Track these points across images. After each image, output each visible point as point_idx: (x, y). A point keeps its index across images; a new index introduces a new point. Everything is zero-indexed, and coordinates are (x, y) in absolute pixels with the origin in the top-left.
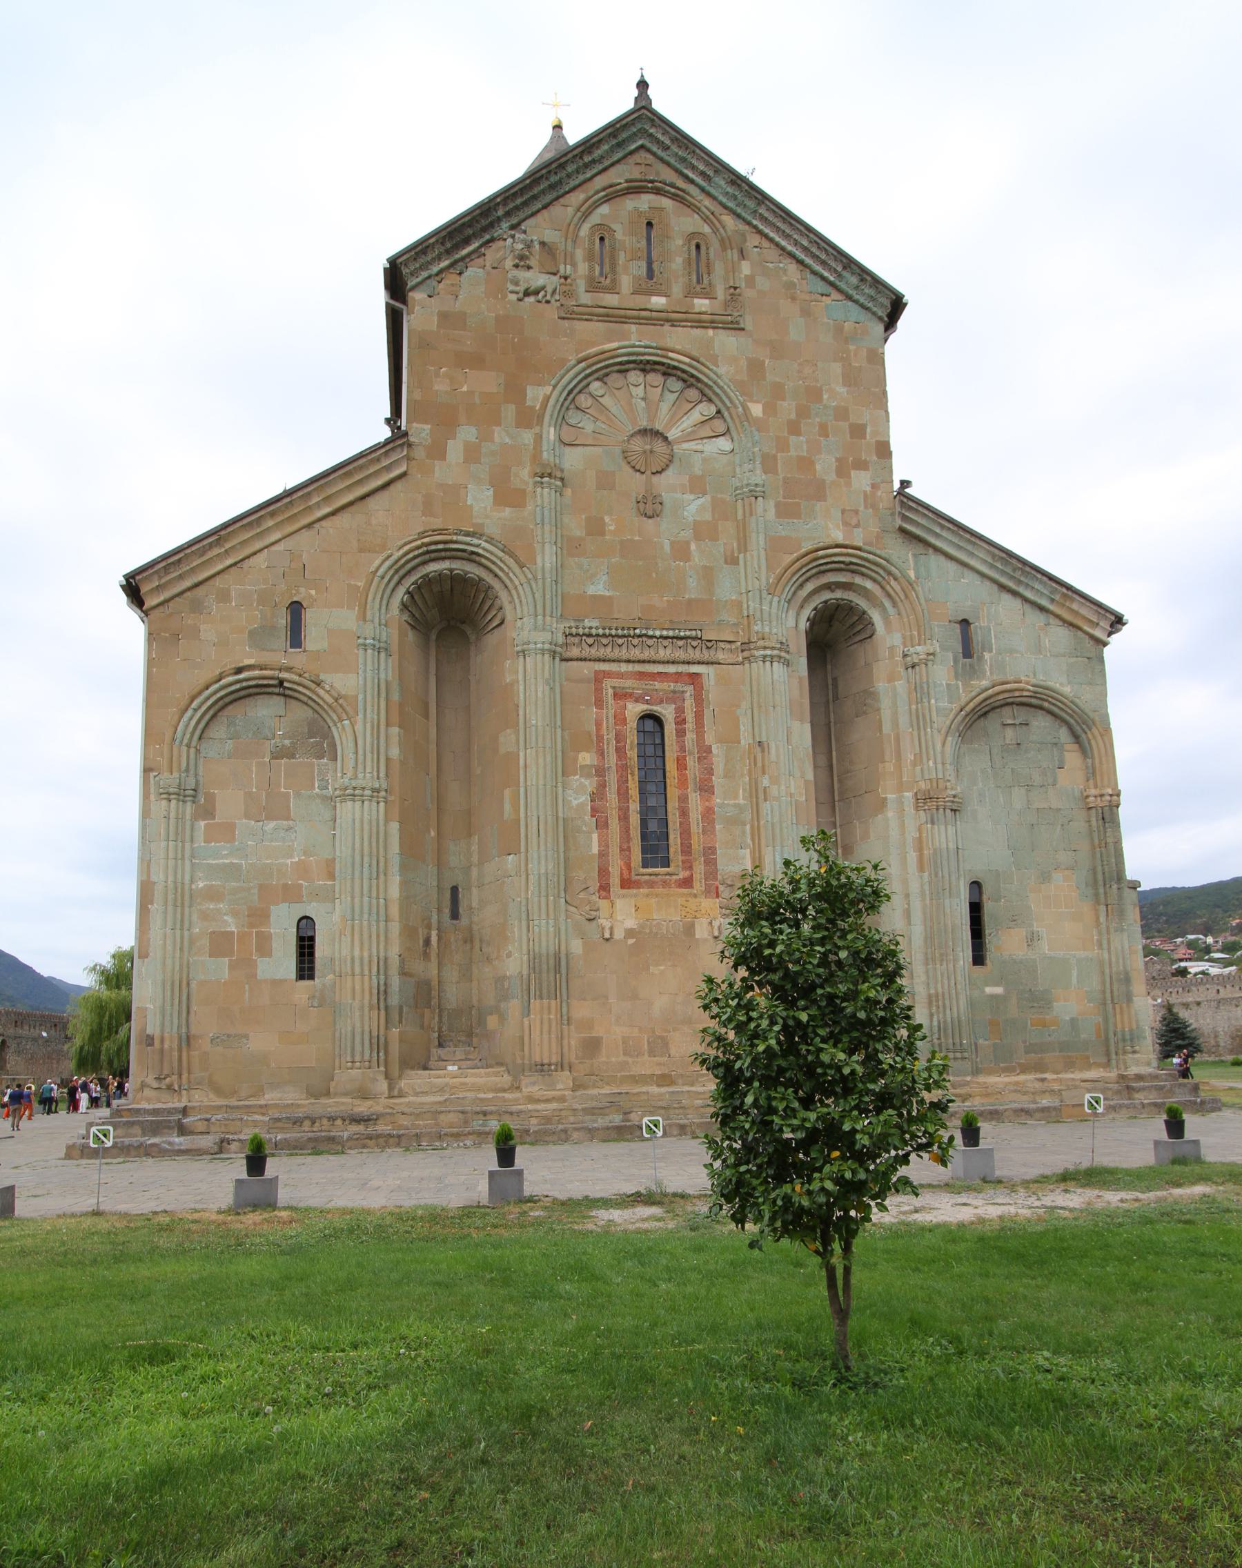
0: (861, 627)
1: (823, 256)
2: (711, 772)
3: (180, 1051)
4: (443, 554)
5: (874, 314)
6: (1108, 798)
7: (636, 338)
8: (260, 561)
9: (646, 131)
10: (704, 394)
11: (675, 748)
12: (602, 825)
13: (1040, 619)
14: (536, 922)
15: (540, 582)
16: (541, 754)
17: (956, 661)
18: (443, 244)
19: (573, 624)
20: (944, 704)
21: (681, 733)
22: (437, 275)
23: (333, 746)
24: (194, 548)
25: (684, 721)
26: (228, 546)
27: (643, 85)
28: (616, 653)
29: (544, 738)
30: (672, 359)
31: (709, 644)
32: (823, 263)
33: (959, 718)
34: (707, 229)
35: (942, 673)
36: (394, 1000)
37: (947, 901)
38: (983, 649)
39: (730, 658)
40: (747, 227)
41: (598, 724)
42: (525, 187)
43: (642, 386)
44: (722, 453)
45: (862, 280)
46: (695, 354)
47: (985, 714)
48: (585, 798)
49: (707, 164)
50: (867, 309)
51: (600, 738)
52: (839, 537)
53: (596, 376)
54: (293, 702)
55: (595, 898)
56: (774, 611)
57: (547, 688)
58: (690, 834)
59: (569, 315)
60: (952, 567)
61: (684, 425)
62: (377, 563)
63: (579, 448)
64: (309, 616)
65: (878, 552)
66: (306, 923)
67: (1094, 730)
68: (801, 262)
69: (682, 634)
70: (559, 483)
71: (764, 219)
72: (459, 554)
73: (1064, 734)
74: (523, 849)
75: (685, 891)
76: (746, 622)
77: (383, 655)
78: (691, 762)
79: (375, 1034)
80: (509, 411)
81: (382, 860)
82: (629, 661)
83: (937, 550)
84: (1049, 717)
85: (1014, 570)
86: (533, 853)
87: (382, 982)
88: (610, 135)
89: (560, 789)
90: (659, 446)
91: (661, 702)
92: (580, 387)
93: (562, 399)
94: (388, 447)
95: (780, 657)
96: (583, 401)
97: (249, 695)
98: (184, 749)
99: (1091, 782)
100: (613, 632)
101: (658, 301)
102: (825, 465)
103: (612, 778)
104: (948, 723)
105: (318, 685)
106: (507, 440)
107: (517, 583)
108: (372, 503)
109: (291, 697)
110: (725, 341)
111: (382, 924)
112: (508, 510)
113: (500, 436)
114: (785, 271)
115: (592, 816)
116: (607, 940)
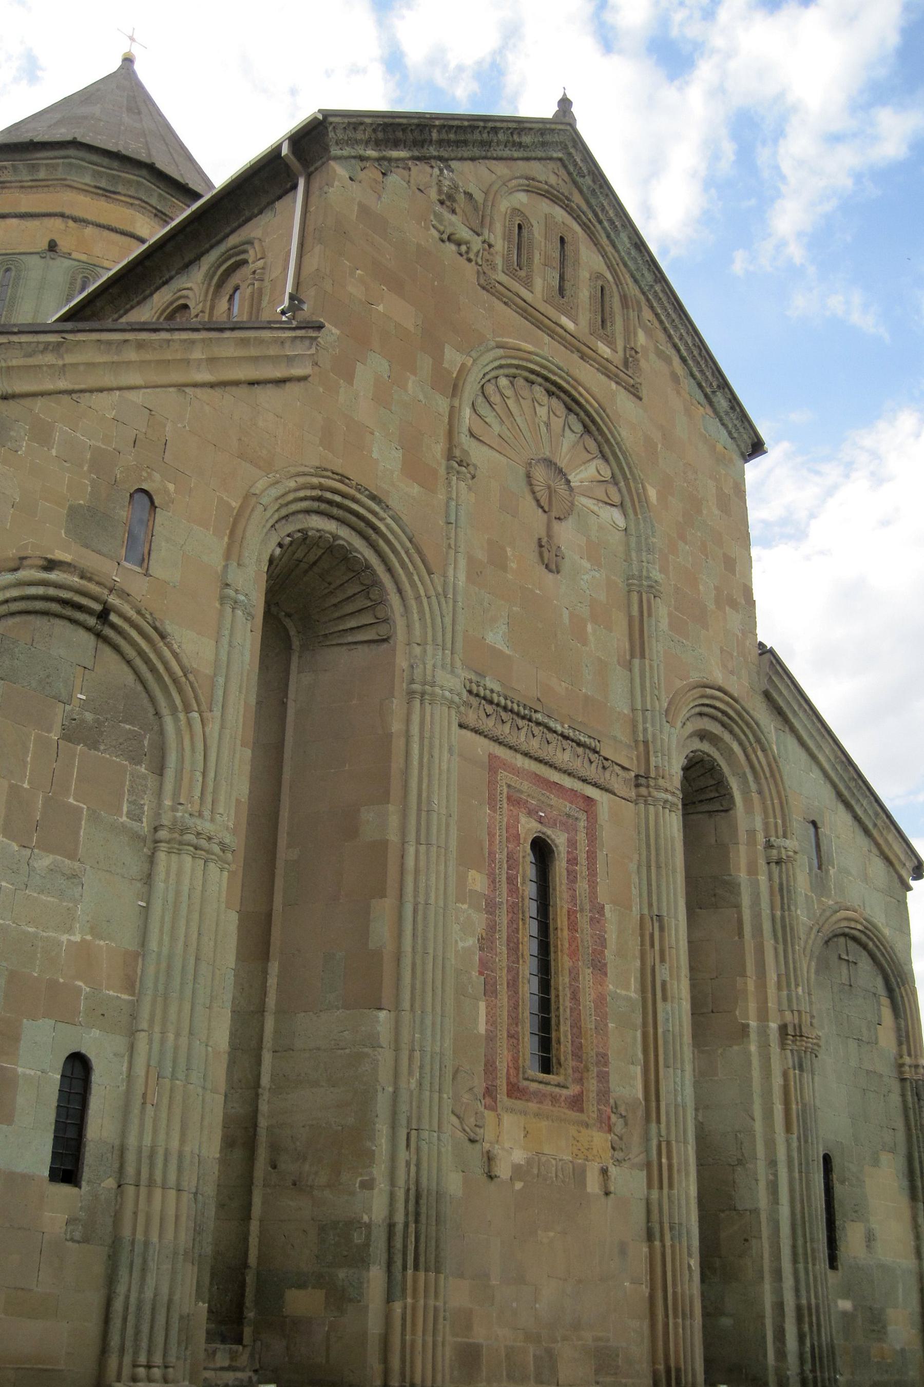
4: (335, 511)
30: (581, 395)
31: (606, 763)
49: (617, 215)
51: (491, 853)
72: (354, 519)
76: (641, 748)
80: (425, 362)
82: (526, 754)
83: (793, 730)
103: (503, 919)
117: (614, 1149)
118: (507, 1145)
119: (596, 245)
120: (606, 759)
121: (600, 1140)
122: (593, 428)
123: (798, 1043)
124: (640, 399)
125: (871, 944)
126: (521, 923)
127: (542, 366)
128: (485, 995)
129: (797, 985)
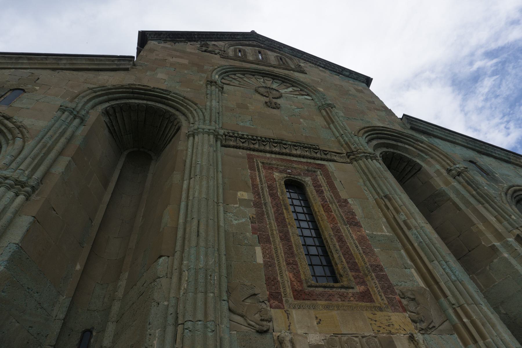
0: (409, 169)
2: (353, 214)
4: (143, 96)
14: (189, 324)
15: (208, 110)
19: (230, 131)
25: (320, 186)
28: (262, 148)
30: (276, 73)
31: (325, 152)
41: (253, 179)
51: (255, 186)
69: (306, 145)
74: (178, 248)
77: (77, 121)
82: (272, 152)
91: (300, 175)
96: (233, 76)
100: (259, 138)
107: (192, 109)
112: (189, 90)
117: (414, 321)
118: (300, 332)
119: (275, 52)
120: (326, 151)
124: (306, 73)
126: (284, 211)
128: (259, 243)
129: (510, 216)
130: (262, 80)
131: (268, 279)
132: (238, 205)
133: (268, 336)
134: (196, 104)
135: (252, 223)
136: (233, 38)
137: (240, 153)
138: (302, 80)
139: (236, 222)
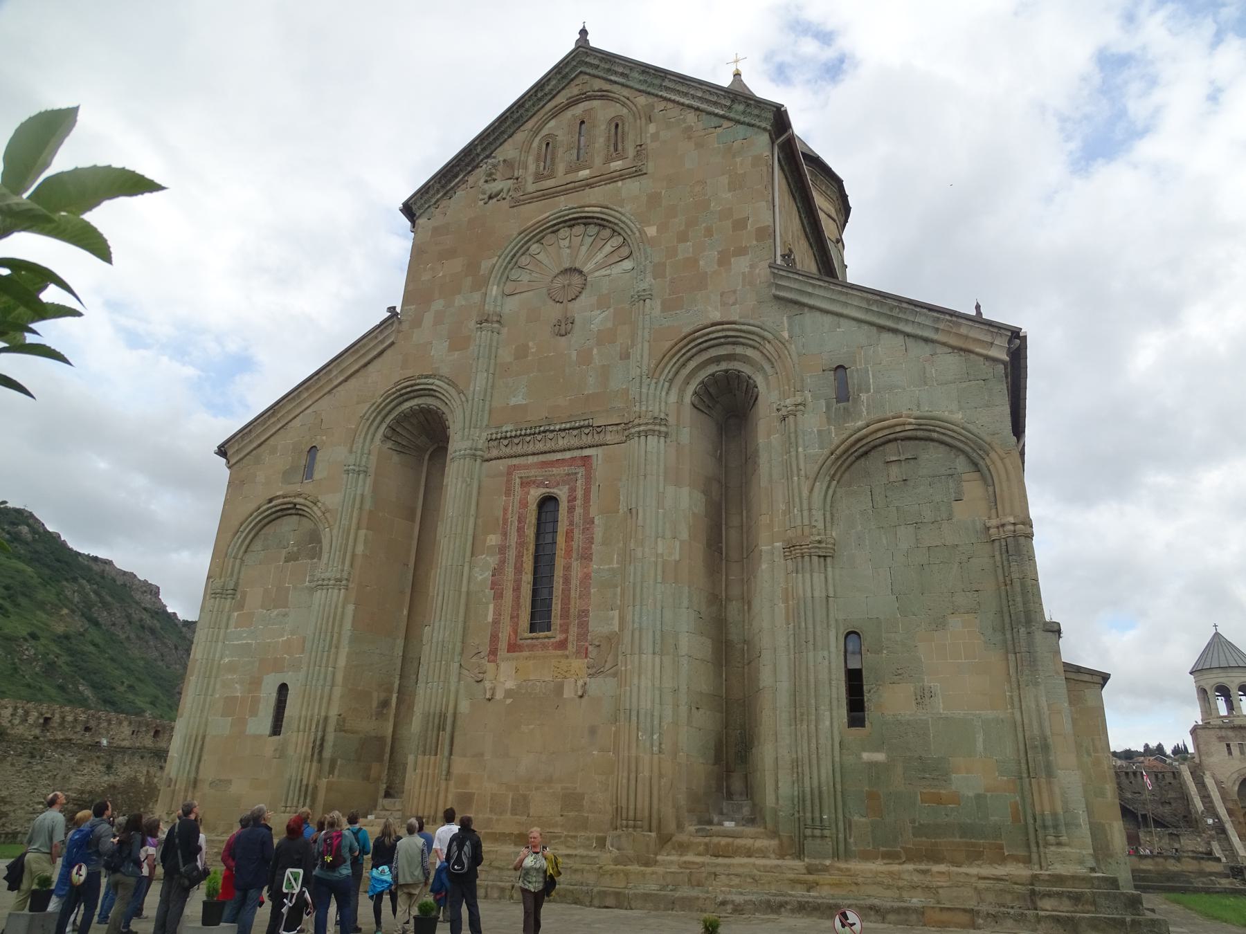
1: (714, 99)
2: (591, 541)
3: (186, 791)
4: (412, 395)
5: (759, 127)
6: (1011, 528)
7: (563, 204)
8: (297, 422)
9: (583, 61)
10: (614, 231)
11: (566, 522)
12: (498, 596)
13: (925, 350)
16: (452, 539)
17: (828, 407)
18: (439, 183)
19: (494, 431)
20: (815, 450)
21: (571, 509)
22: (435, 204)
23: (321, 549)
24: (258, 421)
25: (575, 499)
26: (279, 416)
27: (584, 32)
29: (456, 526)
30: (588, 212)
31: (600, 429)
32: (715, 103)
33: (829, 462)
34: (625, 111)
35: (812, 422)
36: (327, 754)
37: (811, 654)
38: (860, 390)
39: (617, 438)
40: (656, 99)
41: (505, 510)
42: (495, 128)
43: (568, 238)
44: (626, 271)
45: (748, 105)
46: (606, 203)
47: (866, 453)
48: (488, 574)
49: (624, 66)
50: (753, 125)
51: (505, 521)
52: (716, 316)
53: (533, 241)
54: (304, 519)
55: (484, 661)
56: (652, 391)
57: (464, 485)
58: (569, 598)
59: (516, 203)
60: (828, 319)
61: (598, 258)
62: (367, 408)
63: (517, 296)
64: (319, 455)
65: (751, 322)
66: (283, 689)
67: (993, 454)
68: (697, 109)
69: (577, 424)
70: (496, 325)
71: (667, 89)
72: (422, 392)
73: (961, 464)
75: (560, 652)
77: (361, 476)
78: (576, 532)
79: (305, 782)
81: (336, 636)
82: (534, 454)
83: (812, 308)
84: (942, 448)
85: (891, 309)
86: (437, 624)
87: (319, 738)
88: (556, 73)
89: (466, 569)
90: (576, 279)
92: (524, 249)
93: (504, 264)
94: (382, 327)
95: (654, 431)
96: (524, 260)
97: (279, 517)
98: (232, 560)
99: (994, 511)
101: (584, 173)
102: (709, 261)
103: (512, 554)
104: (816, 468)
105: (315, 504)
106: (463, 303)
108: (371, 368)
109: (304, 516)
110: (630, 188)
111: (327, 689)
112: (457, 353)
113: (459, 301)
114: (684, 120)
115: (491, 589)
116: (489, 700)
118: (502, 680)
121: (578, 664)
122: (605, 223)
123: (793, 552)
125: (935, 435)
127: (557, 218)
129: (794, 507)
130: (566, 242)
131: (492, 635)
132: (484, 556)
133: (482, 683)
134: (460, 392)
135: (492, 576)
136: (540, 100)
137: (501, 468)
138: (627, 208)
139: (481, 577)
